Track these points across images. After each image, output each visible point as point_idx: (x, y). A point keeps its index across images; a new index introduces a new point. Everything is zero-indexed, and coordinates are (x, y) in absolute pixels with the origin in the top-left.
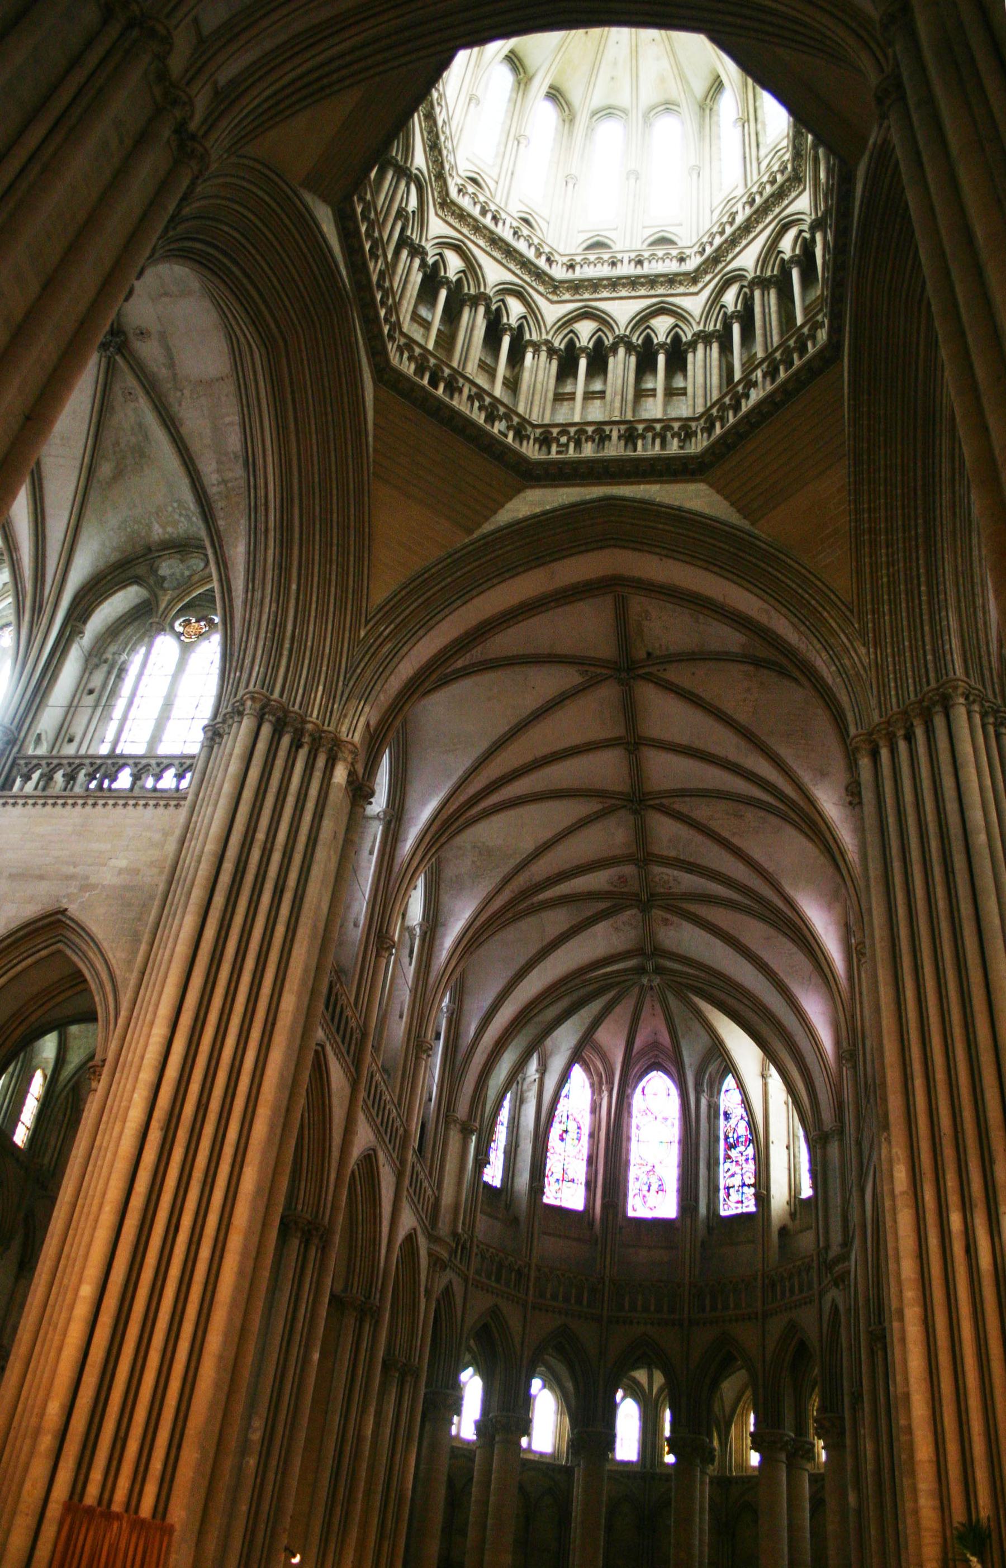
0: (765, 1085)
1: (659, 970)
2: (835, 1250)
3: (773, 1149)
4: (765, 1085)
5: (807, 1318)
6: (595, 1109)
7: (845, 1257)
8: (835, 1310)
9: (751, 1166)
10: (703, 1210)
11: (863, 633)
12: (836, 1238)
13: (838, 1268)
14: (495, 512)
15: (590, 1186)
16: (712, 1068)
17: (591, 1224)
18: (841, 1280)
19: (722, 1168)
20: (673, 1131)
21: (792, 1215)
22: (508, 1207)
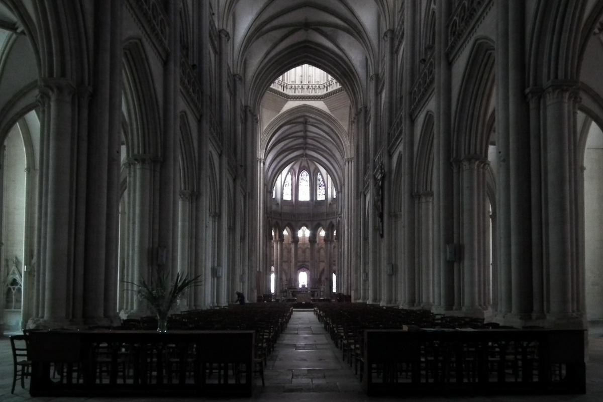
0: (327, 176)
1: (306, 157)
2: (339, 213)
3: (328, 189)
4: (327, 176)
5: (334, 221)
6: (292, 179)
7: (341, 214)
8: (339, 221)
9: (324, 191)
10: (314, 199)
11: (349, 139)
12: (340, 210)
13: (340, 216)
14: (282, 108)
15: (292, 195)
16: (316, 171)
17: (292, 202)
18: (340, 217)
19: (318, 190)
20: (308, 183)
21: (332, 201)
22: (276, 201)
